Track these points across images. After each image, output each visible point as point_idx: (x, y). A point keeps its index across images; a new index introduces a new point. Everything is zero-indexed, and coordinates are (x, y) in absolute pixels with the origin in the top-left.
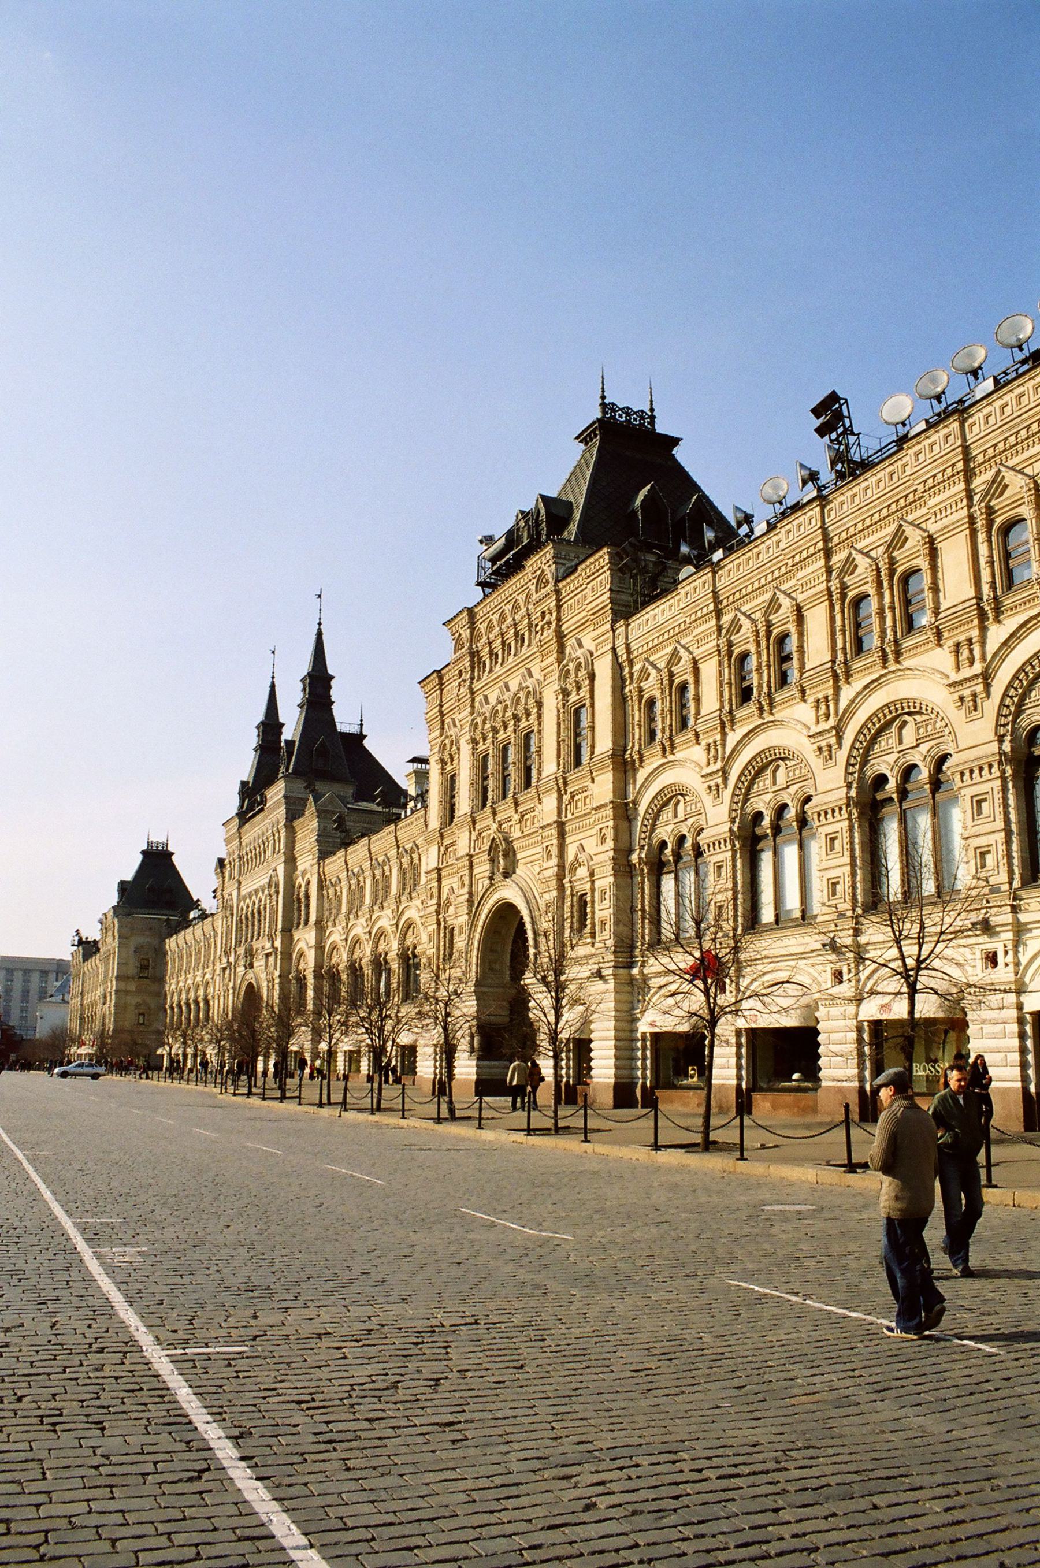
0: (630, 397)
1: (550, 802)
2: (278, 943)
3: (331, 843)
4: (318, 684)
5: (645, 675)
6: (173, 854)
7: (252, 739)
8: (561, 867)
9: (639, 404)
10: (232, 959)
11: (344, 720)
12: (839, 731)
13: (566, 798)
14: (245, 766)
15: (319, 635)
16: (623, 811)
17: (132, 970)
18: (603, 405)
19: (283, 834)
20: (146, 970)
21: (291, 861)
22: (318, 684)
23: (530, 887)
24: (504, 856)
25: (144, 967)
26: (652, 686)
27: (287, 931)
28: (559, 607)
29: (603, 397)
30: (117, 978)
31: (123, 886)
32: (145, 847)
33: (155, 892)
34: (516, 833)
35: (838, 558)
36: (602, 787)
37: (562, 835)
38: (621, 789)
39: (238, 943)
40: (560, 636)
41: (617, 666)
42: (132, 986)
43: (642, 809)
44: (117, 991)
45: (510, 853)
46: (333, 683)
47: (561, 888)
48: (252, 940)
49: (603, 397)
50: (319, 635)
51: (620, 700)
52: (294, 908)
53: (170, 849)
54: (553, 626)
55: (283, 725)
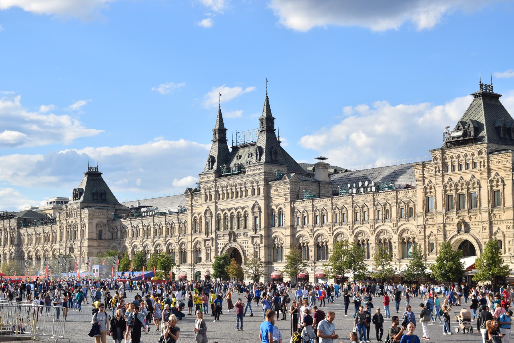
0: (486, 81)
2: (262, 232)
6: (102, 174)
9: (489, 83)
10: (213, 236)
13: (492, 215)
14: (211, 148)
17: (95, 235)
18: (481, 86)
19: (262, 188)
21: (268, 199)
25: (100, 233)
28: (488, 162)
29: (480, 82)
30: (89, 239)
32: (87, 171)
34: (467, 220)
39: (218, 229)
40: (489, 171)
42: (95, 244)
45: (467, 225)
46: (275, 121)
49: (480, 82)
52: (272, 218)
53: (100, 171)
54: (486, 166)
55: (226, 130)
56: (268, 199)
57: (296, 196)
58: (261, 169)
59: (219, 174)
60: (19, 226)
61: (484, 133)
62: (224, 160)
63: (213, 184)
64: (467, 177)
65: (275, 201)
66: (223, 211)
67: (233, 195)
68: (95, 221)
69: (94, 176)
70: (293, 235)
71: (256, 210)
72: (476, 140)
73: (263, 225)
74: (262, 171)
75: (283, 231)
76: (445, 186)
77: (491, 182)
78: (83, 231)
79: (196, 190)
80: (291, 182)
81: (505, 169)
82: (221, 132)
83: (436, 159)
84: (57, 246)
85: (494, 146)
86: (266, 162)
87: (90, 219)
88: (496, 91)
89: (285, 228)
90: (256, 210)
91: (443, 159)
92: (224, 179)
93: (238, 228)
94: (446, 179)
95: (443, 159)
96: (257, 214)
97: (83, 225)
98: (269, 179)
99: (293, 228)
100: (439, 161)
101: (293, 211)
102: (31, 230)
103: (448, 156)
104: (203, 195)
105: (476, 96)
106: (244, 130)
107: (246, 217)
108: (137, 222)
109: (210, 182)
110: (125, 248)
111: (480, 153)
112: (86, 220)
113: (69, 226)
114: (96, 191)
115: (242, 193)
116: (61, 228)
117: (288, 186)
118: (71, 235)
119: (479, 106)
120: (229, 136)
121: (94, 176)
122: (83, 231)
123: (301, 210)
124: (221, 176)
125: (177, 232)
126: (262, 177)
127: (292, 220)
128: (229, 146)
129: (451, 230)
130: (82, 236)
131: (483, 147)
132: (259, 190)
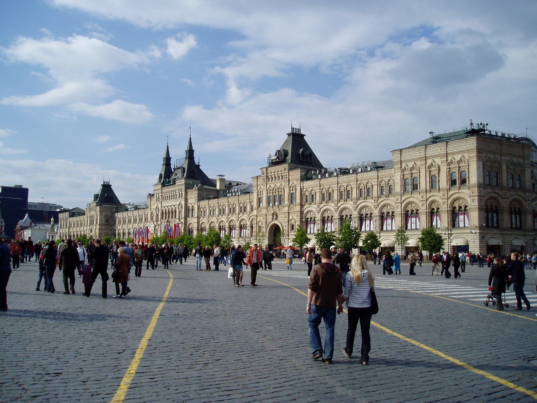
1: (286, 208)
2: (183, 221)
3: (201, 198)
4: (190, 153)
5: (306, 191)
7: (162, 162)
8: (289, 219)
10: (159, 223)
11: (196, 161)
12: (338, 209)
14: (160, 169)
15: (190, 139)
16: (302, 212)
17: (103, 222)
19: (184, 193)
20: (109, 223)
21: (186, 200)
22: (190, 153)
23: (282, 222)
24: (275, 216)
25: (107, 221)
26: (307, 193)
27: (185, 218)
31: (96, 197)
33: (107, 197)
34: (278, 212)
35: (339, 185)
36: (298, 208)
37: (289, 214)
38: (301, 209)
40: (289, 180)
41: (301, 189)
42: (104, 227)
43: (305, 212)
44: (99, 229)
45: (277, 215)
47: (289, 223)
48: (169, 218)
50: (190, 139)
51: (301, 195)
56: (186, 200)
57: (201, 198)
58: (183, 181)
59: (163, 185)
60: (70, 216)
61: (289, 157)
62: (167, 177)
63: (160, 191)
64: (278, 185)
65: (189, 201)
66: (164, 207)
67: (169, 198)
68: (104, 214)
69: (107, 188)
70: (198, 223)
71: (180, 207)
72: (283, 161)
73: (183, 216)
74: (184, 183)
75: (193, 220)
76: (267, 190)
77: (290, 187)
78: (97, 220)
79: (153, 195)
80: (199, 190)
81: (297, 180)
82: (168, 160)
83: (263, 173)
84: (85, 228)
85: (294, 165)
86: (187, 177)
87: (100, 212)
88: (302, 133)
89: (195, 218)
90: (180, 207)
91: (267, 173)
92: (166, 187)
93: (172, 218)
94: (268, 186)
95: (267, 173)
96: (180, 209)
97: (97, 217)
98: (188, 187)
99: (198, 218)
100: (265, 175)
101: (198, 208)
102: (74, 219)
103: (269, 171)
104: (156, 198)
105: (289, 135)
106: (179, 158)
107: (176, 212)
108: (125, 214)
109: (159, 189)
110: (115, 230)
111: (285, 169)
112: (98, 213)
113: (91, 217)
114: (107, 197)
115: (174, 197)
116: (87, 217)
117: (197, 192)
118: (92, 223)
119: (290, 141)
120: (172, 162)
121: (107, 188)
122: (97, 220)
123: (203, 207)
124: (165, 186)
125: (144, 221)
126: (184, 187)
127: (198, 213)
128: (172, 167)
129: (270, 218)
130: (97, 223)
131: (286, 166)
132: (182, 194)
